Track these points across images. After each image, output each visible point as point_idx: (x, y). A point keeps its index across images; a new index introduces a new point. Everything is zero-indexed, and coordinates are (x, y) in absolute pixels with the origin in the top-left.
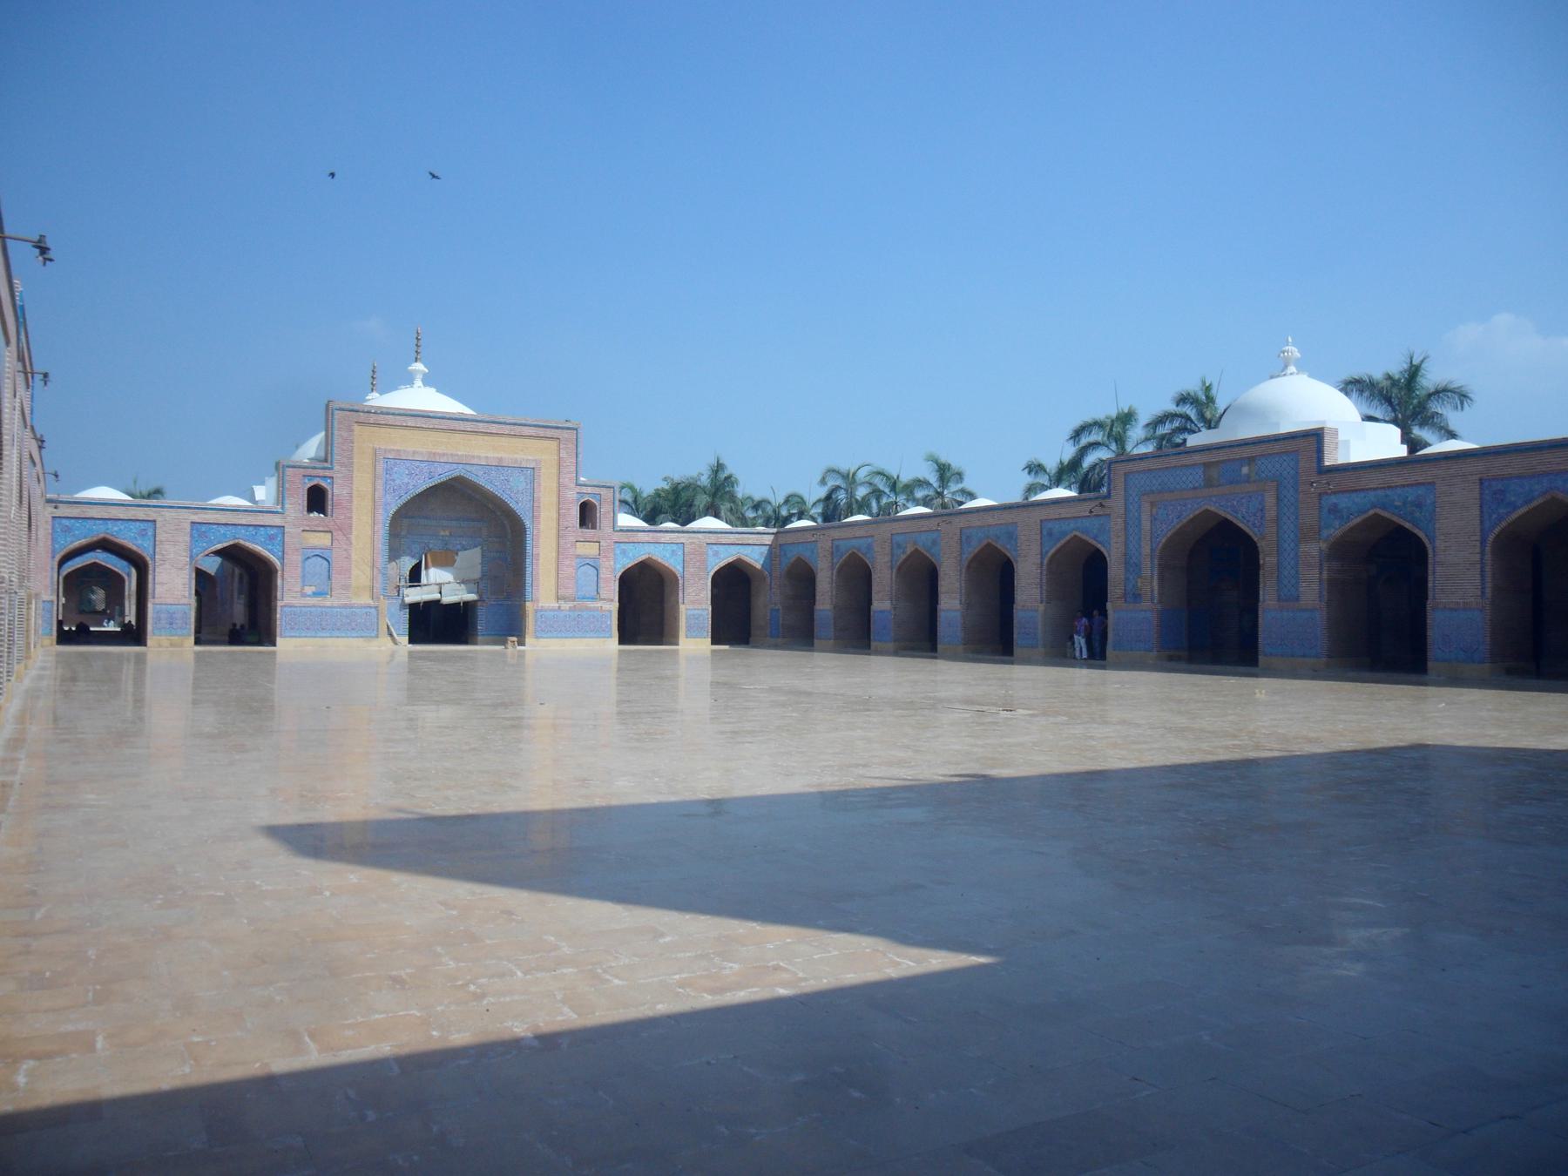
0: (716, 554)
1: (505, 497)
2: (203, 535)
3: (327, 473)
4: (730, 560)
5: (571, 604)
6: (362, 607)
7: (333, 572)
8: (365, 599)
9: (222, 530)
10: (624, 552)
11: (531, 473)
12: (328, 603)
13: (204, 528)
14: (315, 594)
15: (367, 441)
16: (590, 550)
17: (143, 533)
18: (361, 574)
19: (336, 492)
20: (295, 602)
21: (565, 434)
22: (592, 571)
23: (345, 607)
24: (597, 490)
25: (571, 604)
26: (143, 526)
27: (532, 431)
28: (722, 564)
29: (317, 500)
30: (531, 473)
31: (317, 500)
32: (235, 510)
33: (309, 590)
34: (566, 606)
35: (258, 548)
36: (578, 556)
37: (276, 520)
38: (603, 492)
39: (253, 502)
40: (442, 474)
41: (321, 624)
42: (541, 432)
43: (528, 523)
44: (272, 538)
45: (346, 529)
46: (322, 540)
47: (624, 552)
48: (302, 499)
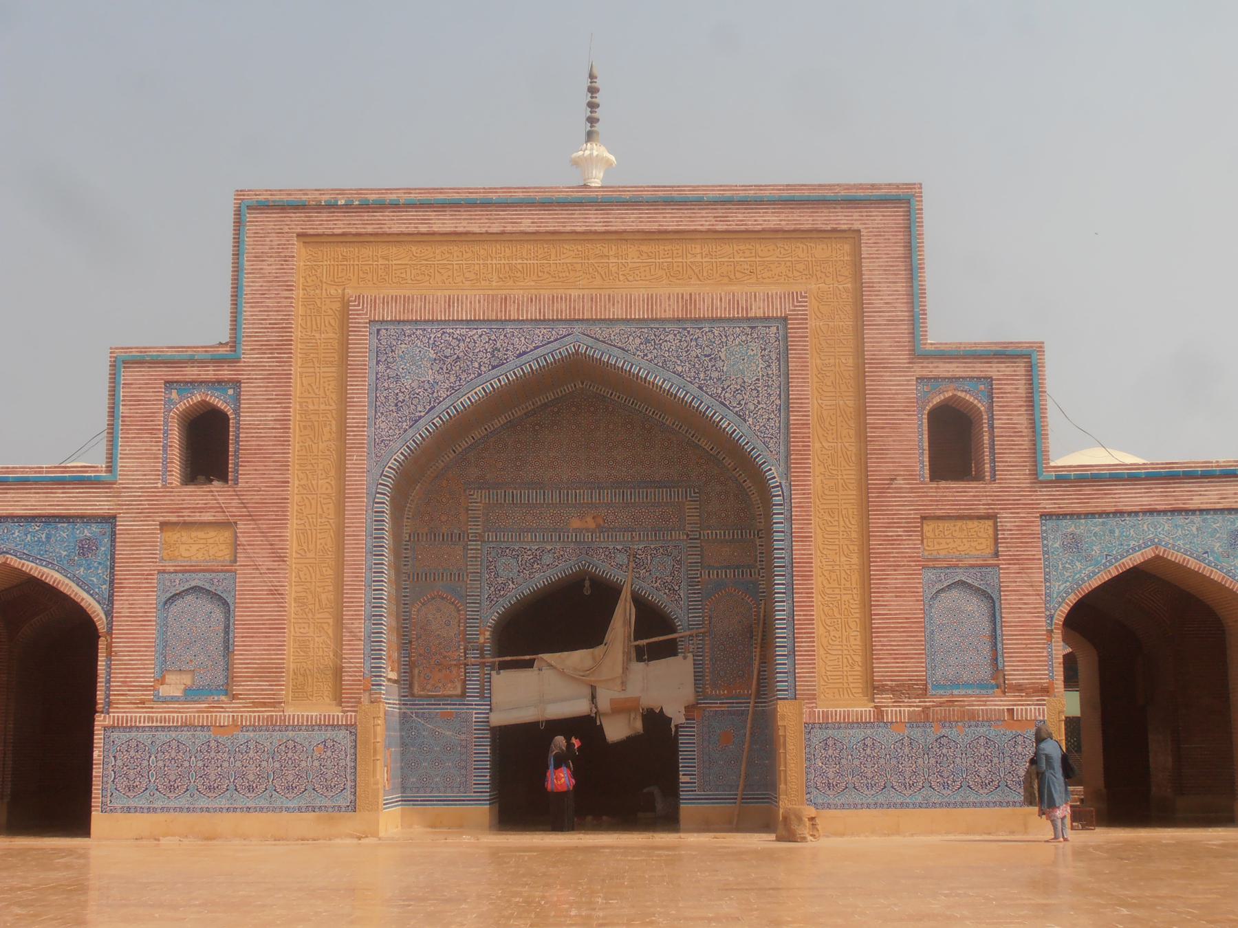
1: (706, 404)
3: (226, 373)
7: (238, 633)
8: (322, 708)
10: (1074, 544)
11: (779, 334)
12: (224, 718)
14: (191, 694)
16: (968, 542)
18: (304, 638)
19: (251, 423)
20: (140, 716)
21: (872, 222)
22: (974, 607)
23: (271, 726)
24: (979, 369)
29: (207, 446)
30: (779, 334)
31: (207, 446)
33: (173, 687)
34: (899, 710)
35: (53, 576)
37: (100, 504)
38: (995, 370)
40: (528, 354)
41: (212, 777)
42: (805, 219)
43: (774, 472)
44: (86, 548)
47: (1074, 544)
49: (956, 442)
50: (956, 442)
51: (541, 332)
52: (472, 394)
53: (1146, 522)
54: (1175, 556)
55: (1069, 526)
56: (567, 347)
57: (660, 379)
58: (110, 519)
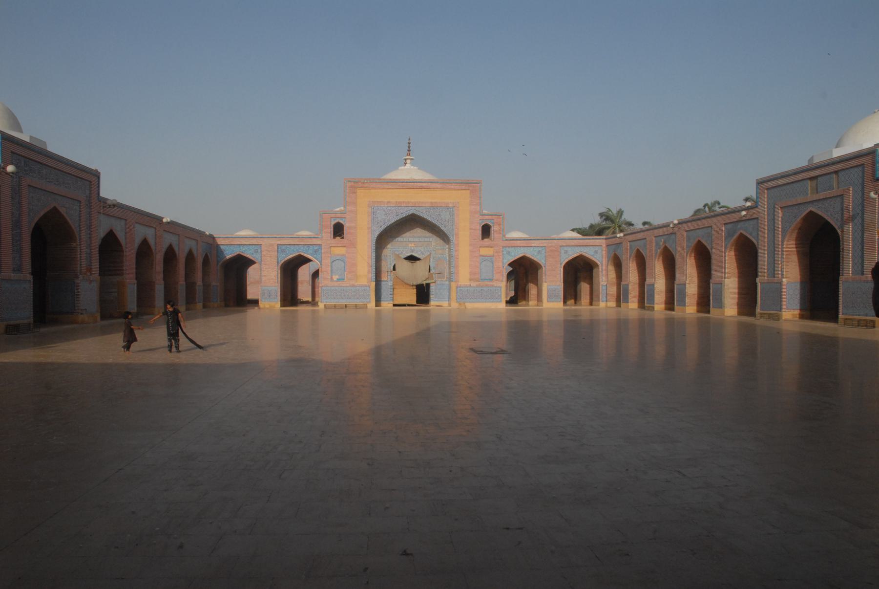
0: (566, 252)
1: (438, 224)
2: (283, 251)
4: (575, 255)
5: (477, 283)
6: (362, 286)
9: (292, 248)
10: (509, 253)
13: (284, 247)
14: (338, 280)
15: (364, 198)
17: (256, 251)
23: (353, 286)
25: (477, 283)
26: (256, 247)
27: (453, 186)
28: (570, 258)
29: (338, 230)
31: (338, 230)
32: (303, 237)
33: (335, 278)
34: (474, 284)
36: (483, 256)
37: (318, 242)
39: (306, 234)
40: (404, 213)
44: (316, 251)
45: (353, 245)
46: (341, 251)
47: (509, 253)
48: (330, 231)
49: (486, 231)
50: (486, 231)
51: (406, 209)
52: (393, 221)
53: (522, 249)
54: (528, 255)
55: (508, 249)
56: (411, 212)
57: (429, 219)
58: (320, 245)
